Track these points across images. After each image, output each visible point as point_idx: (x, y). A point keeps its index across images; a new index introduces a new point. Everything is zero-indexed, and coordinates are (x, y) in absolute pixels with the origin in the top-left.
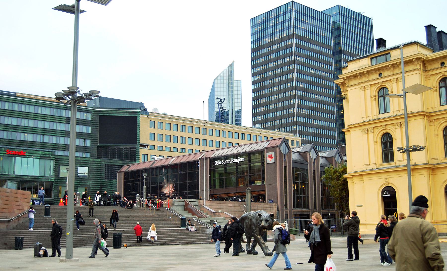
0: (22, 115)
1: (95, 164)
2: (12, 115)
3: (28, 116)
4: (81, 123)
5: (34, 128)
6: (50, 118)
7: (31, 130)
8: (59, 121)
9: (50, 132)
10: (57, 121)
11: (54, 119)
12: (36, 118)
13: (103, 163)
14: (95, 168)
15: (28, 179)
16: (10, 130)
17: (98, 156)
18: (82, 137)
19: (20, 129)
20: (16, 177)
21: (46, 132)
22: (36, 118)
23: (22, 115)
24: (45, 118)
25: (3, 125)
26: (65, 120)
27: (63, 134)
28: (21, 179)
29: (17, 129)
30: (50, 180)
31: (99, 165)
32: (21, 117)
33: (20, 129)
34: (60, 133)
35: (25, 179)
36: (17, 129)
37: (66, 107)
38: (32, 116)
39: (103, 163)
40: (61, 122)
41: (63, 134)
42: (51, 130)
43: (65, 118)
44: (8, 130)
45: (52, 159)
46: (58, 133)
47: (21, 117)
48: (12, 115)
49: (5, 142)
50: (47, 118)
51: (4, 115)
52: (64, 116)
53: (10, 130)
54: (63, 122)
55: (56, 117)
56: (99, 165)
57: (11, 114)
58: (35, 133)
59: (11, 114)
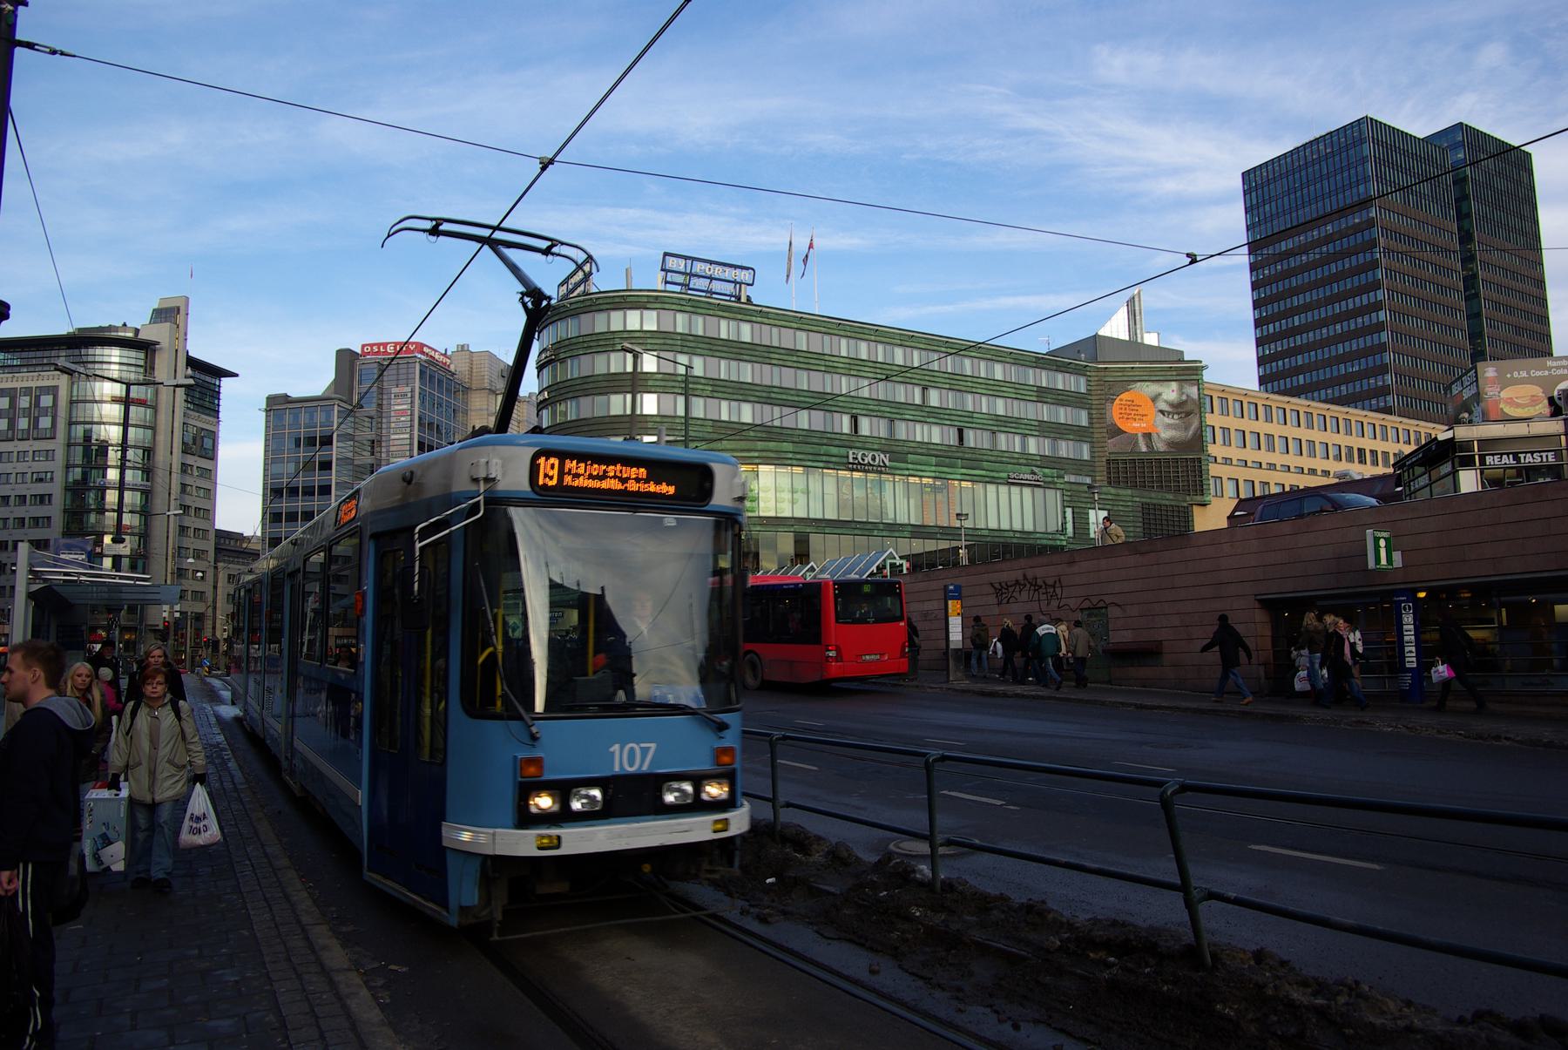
0: (947, 381)
1: (1121, 503)
2: (929, 381)
3: (961, 383)
4: (1067, 401)
5: (975, 415)
6: (1004, 389)
7: (970, 420)
8: (1024, 397)
9: (1009, 425)
10: (1019, 396)
11: (1013, 390)
12: (976, 388)
13: (1138, 499)
14: (1121, 513)
15: (1015, 541)
16: (928, 420)
17: (1110, 483)
18: (1071, 437)
19: (946, 417)
20: (992, 535)
21: (999, 423)
22: (976, 388)
23: (947, 381)
24: (995, 388)
25: (913, 407)
26: (1035, 394)
27: (1033, 428)
28: (1002, 540)
29: (942, 416)
30: (1058, 543)
31: (1130, 504)
32: (947, 386)
33: (946, 417)
34: (1028, 427)
35: (1009, 540)
36: (942, 416)
37: (1034, 360)
38: (970, 384)
39: (1138, 499)
40: (1028, 398)
41: (1033, 428)
42: (1010, 420)
43: (1035, 389)
44: (922, 419)
45: (1058, 486)
46: (1023, 426)
47: (947, 386)
48: (929, 381)
49: (920, 451)
50: (998, 388)
51: (913, 381)
52: (1031, 383)
53: (928, 420)
54: (1031, 398)
55: (1017, 386)
56: (1130, 504)
57: (927, 378)
58: (977, 426)
59: (927, 378)
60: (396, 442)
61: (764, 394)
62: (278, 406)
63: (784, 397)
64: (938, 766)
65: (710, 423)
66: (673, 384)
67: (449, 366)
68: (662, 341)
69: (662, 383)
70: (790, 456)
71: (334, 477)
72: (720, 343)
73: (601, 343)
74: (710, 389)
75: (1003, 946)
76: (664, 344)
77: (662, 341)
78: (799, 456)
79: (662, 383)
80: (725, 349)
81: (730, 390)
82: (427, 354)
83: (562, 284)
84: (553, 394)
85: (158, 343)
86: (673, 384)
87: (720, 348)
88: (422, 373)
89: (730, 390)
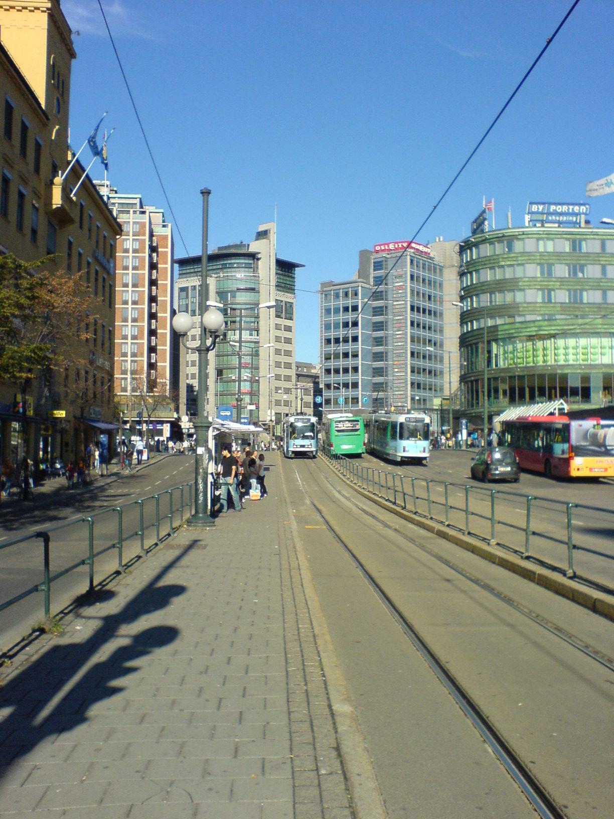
60: (397, 307)
61: (595, 284)
62: (327, 290)
63: (609, 284)
64: (533, 502)
65: (559, 305)
66: (535, 283)
67: (429, 254)
68: (527, 258)
69: (528, 283)
70: (600, 326)
71: (360, 331)
72: (565, 254)
73: (492, 262)
74: (559, 284)
75: (354, 508)
76: (529, 259)
77: (527, 258)
78: (606, 327)
79: (528, 283)
80: (568, 258)
81: (572, 284)
82: (414, 248)
83: (474, 222)
84: (466, 292)
85: (259, 253)
86: (535, 283)
87: (565, 258)
88: (412, 261)
89: (572, 284)
